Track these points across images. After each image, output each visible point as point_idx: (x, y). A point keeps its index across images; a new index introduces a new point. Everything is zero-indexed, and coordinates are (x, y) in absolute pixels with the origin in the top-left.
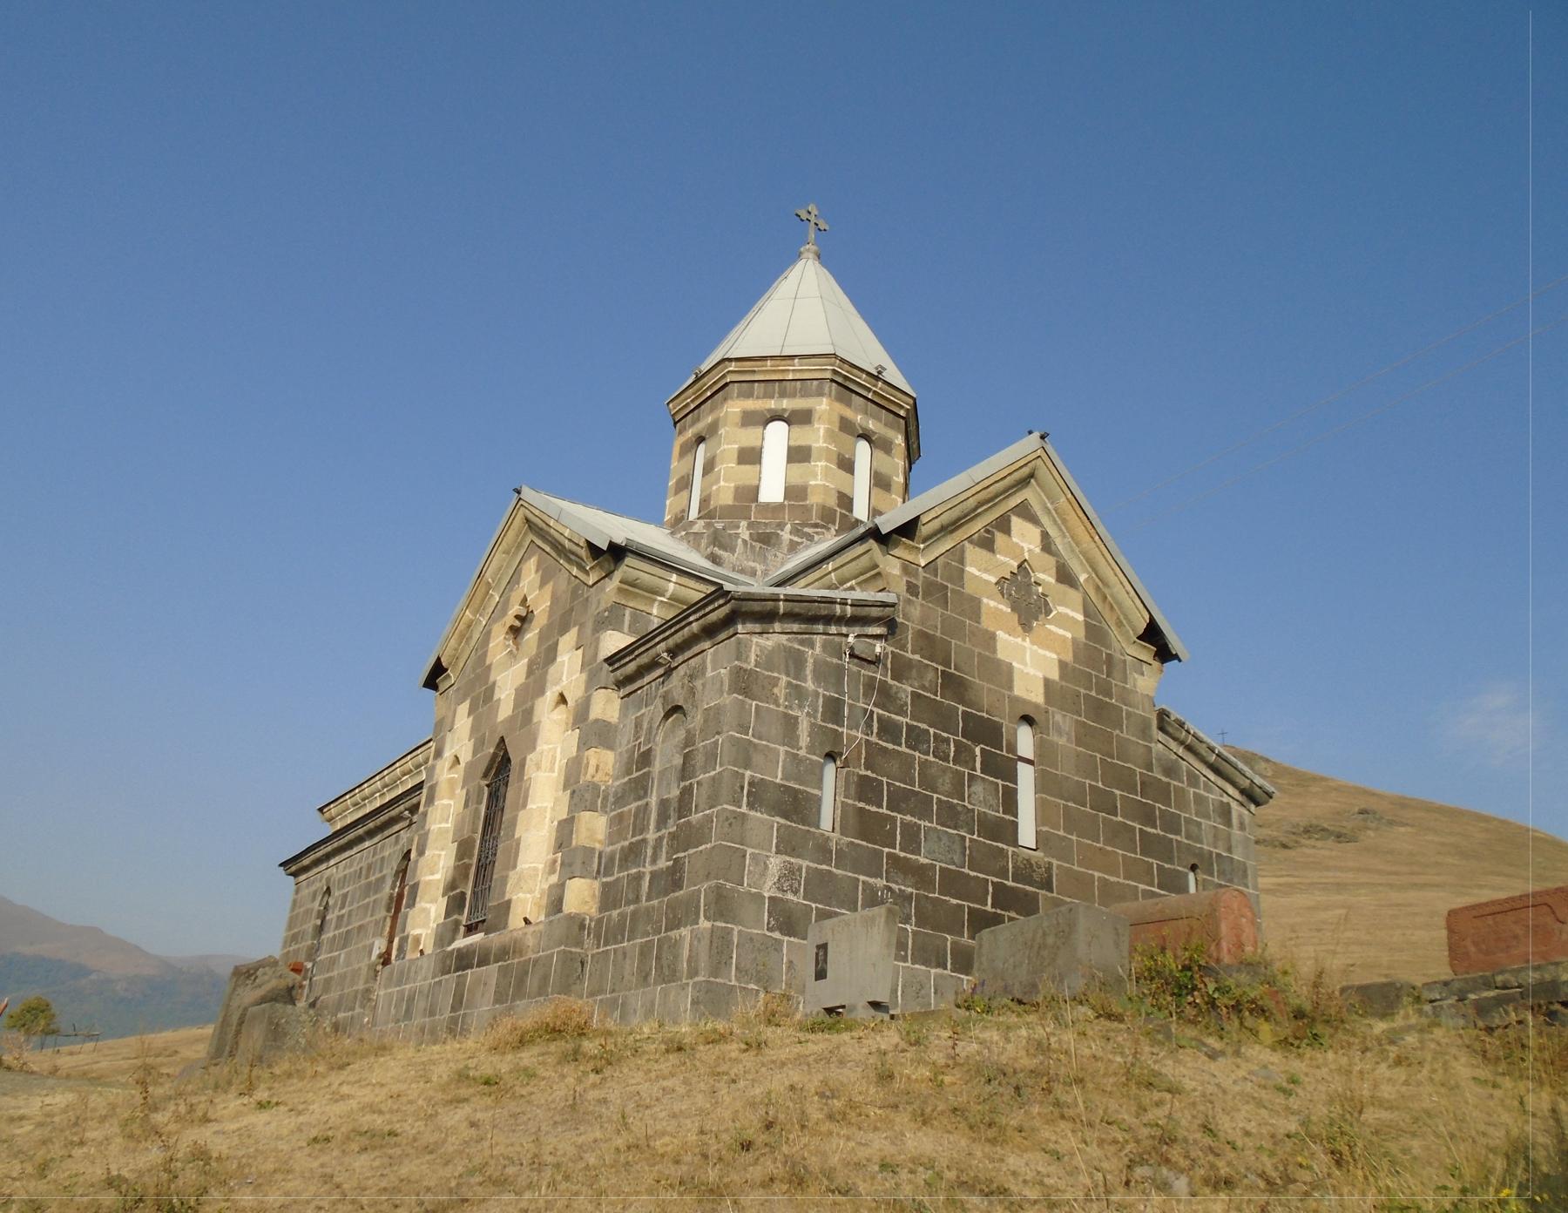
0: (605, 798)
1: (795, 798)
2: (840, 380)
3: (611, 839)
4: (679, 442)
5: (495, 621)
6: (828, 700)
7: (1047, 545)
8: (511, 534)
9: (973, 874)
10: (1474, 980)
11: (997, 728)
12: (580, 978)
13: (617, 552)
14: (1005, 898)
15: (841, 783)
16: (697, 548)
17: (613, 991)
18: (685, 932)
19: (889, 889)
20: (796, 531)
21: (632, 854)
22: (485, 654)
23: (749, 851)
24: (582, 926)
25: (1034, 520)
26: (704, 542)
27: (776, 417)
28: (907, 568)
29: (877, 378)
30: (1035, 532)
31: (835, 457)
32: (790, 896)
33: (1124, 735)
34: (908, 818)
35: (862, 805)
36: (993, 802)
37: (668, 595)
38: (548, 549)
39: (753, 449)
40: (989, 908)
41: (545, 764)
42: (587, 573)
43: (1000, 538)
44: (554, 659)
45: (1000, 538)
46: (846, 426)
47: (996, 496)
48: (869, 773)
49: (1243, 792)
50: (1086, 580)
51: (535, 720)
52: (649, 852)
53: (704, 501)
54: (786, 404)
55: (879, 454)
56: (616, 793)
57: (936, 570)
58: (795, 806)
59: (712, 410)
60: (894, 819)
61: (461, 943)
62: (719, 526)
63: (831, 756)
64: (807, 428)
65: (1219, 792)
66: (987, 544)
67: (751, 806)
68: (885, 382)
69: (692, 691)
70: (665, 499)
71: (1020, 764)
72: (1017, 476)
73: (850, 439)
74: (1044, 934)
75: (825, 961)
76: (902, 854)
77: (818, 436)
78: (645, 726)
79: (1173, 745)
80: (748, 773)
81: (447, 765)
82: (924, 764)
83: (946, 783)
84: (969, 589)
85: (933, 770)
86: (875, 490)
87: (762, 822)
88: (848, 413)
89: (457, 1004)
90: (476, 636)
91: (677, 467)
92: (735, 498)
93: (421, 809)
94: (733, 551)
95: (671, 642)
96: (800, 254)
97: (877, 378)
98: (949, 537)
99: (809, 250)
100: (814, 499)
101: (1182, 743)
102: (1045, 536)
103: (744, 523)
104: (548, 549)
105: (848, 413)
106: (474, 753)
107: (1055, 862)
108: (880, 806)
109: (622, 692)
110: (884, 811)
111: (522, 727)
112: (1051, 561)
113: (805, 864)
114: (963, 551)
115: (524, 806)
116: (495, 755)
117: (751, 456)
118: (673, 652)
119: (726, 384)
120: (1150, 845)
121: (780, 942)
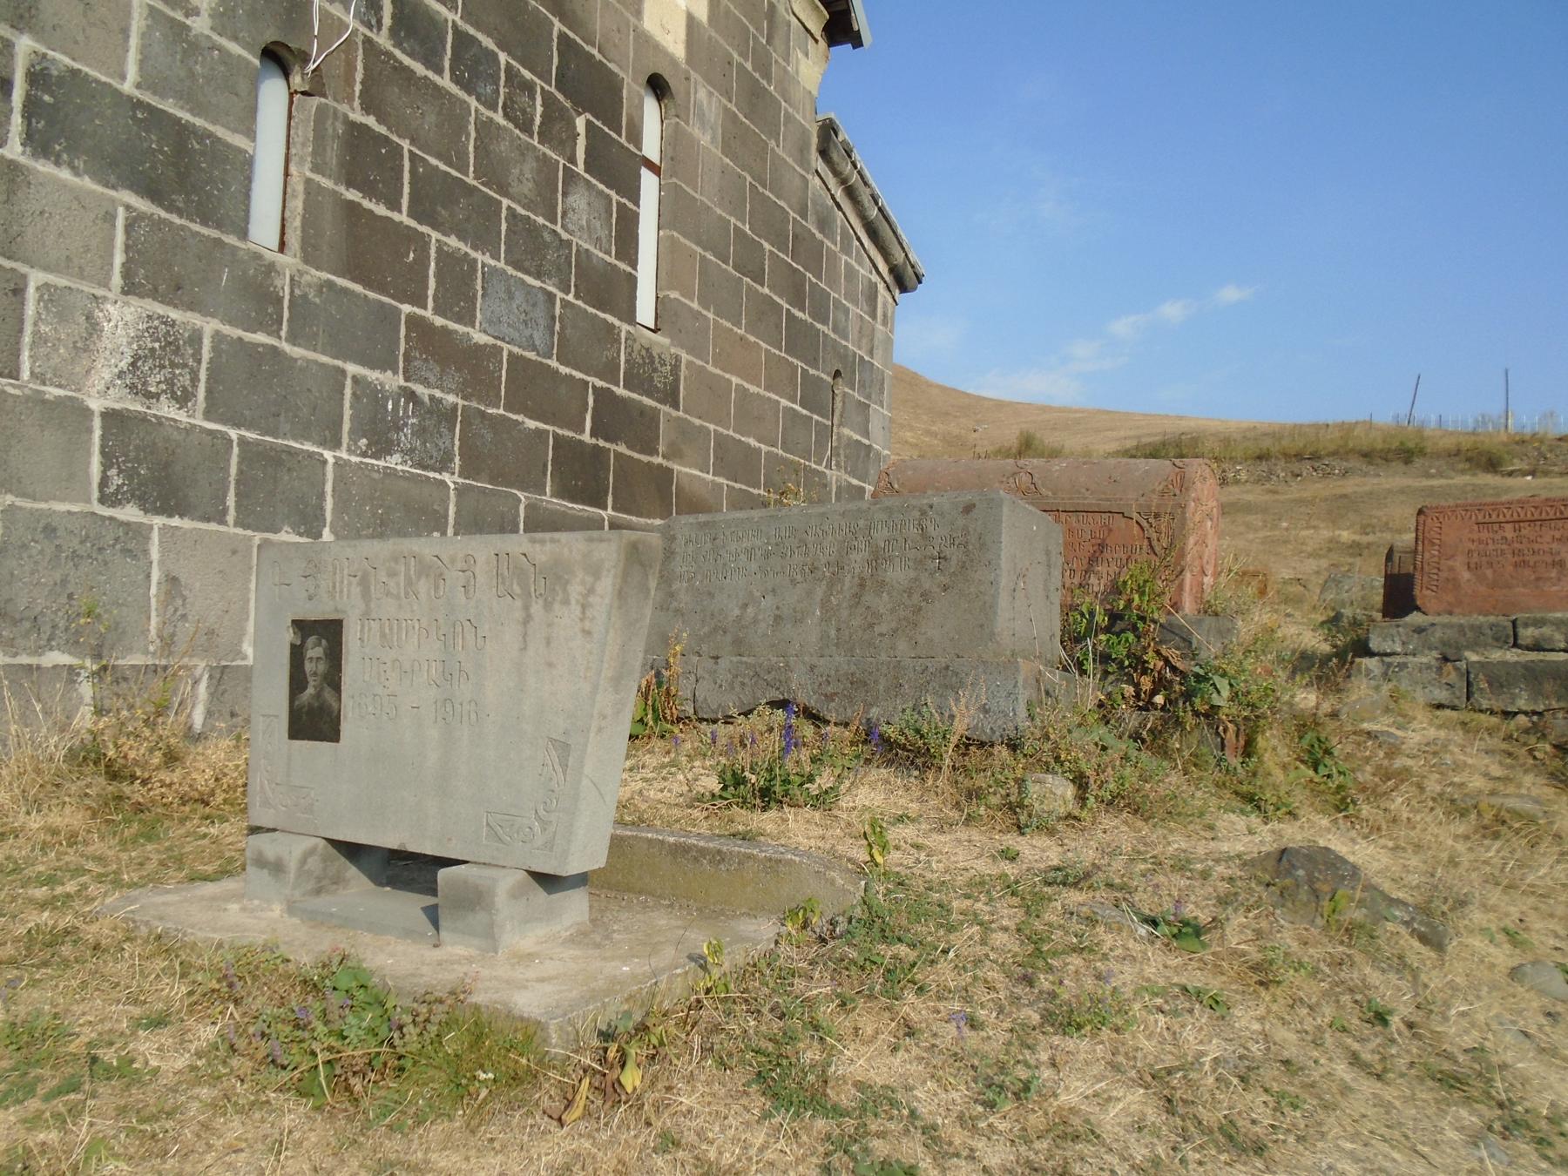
1: (181, 149)
9: (564, 370)
10: (1478, 630)
11: (613, 87)
14: (615, 418)
15: (305, 132)
19: (412, 396)
23: (36, 278)
32: (167, 409)
33: (780, 151)
34: (453, 242)
35: (353, 195)
36: (603, 233)
40: (586, 437)
48: (371, 121)
49: (893, 270)
58: (182, 170)
60: (423, 240)
63: (277, 57)
65: (867, 267)
67: (37, 142)
71: (646, 174)
74: (877, 558)
75: (333, 679)
76: (439, 321)
79: (832, 182)
80: (25, 45)
82: (485, 127)
83: (524, 177)
85: (504, 147)
87: (78, 196)
101: (843, 181)
107: (685, 356)
108: (396, 207)
110: (403, 218)
113: (210, 326)
120: (802, 341)
121: (139, 533)
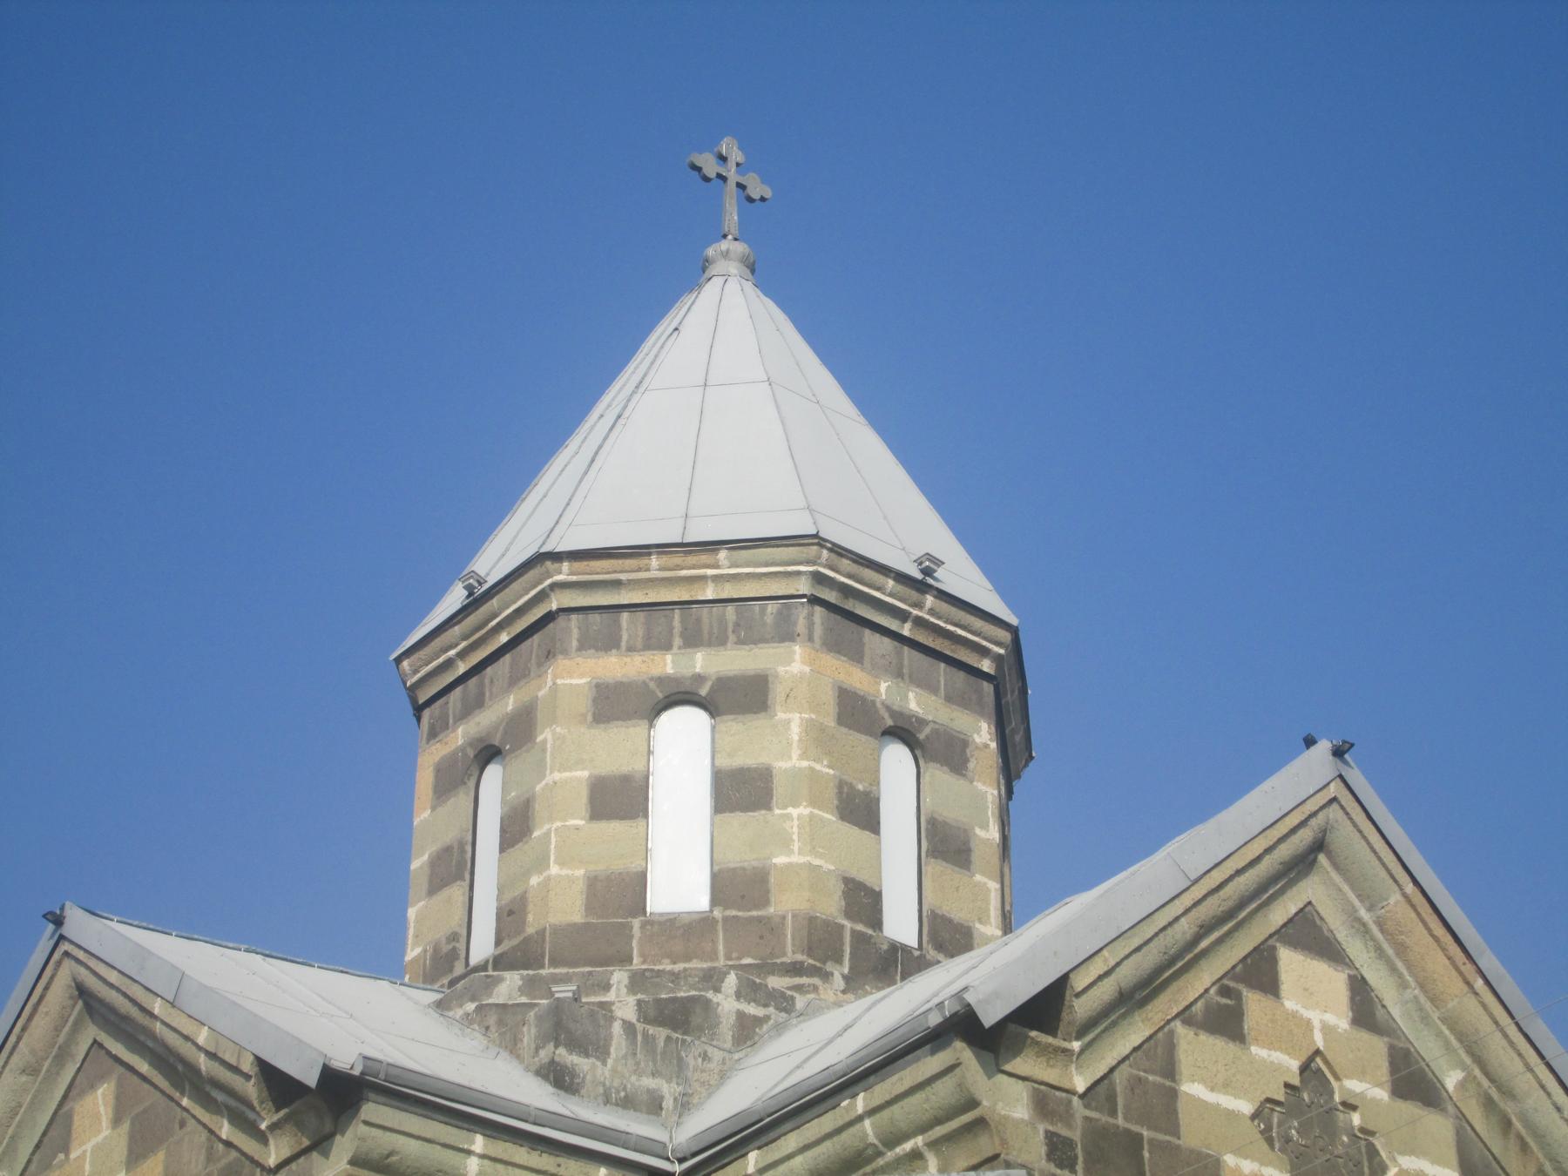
2: (831, 596)
4: (430, 757)
7: (1365, 1009)
8: (41, 1025)
13: (340, 1094)
16: (511, 1045)
20: (750, 990)
25: (1329, 950)
26: (529, 1034)
27: (679, 695)
28: (1047, 1101)
29: (921, 587)
30: (1334, 981)
31: (831, 793)
38: (144, 1067)
39: (626, 779)
42: (262, 1138)
43: (1254, 1004)
45: (1254, 1004)
46: (854, 711)
47: (1241, 905)
50: (1461, 1085)
53: (510, 915)
54: (702, 663)
55: (937, 775)
57: (1111, 1098)
59: (514, 681)
62: (564, 991)
64: (757, 723)
66: (1225, 1021)
68: (943, 595)
70: (405, 911)
72: (1285, 851)
73: (860, 742)
77: (786, 741)
84: (1191, 1136)
86: (933, 867)
88: (857, 679)
91: (431, 823)
92: (589, 908)
94: (598, 1049)
96: (705, 264)
97: (921, 587)
98: (1137, 1017)
99: (727, 254)
100: (787, 903)
102: (1360, 990)
103: (619, 977)
105: (857, 679)
112: (1377, 1047)
114: (1171, 1047)
117: (622, 798)
119: (549, 617)
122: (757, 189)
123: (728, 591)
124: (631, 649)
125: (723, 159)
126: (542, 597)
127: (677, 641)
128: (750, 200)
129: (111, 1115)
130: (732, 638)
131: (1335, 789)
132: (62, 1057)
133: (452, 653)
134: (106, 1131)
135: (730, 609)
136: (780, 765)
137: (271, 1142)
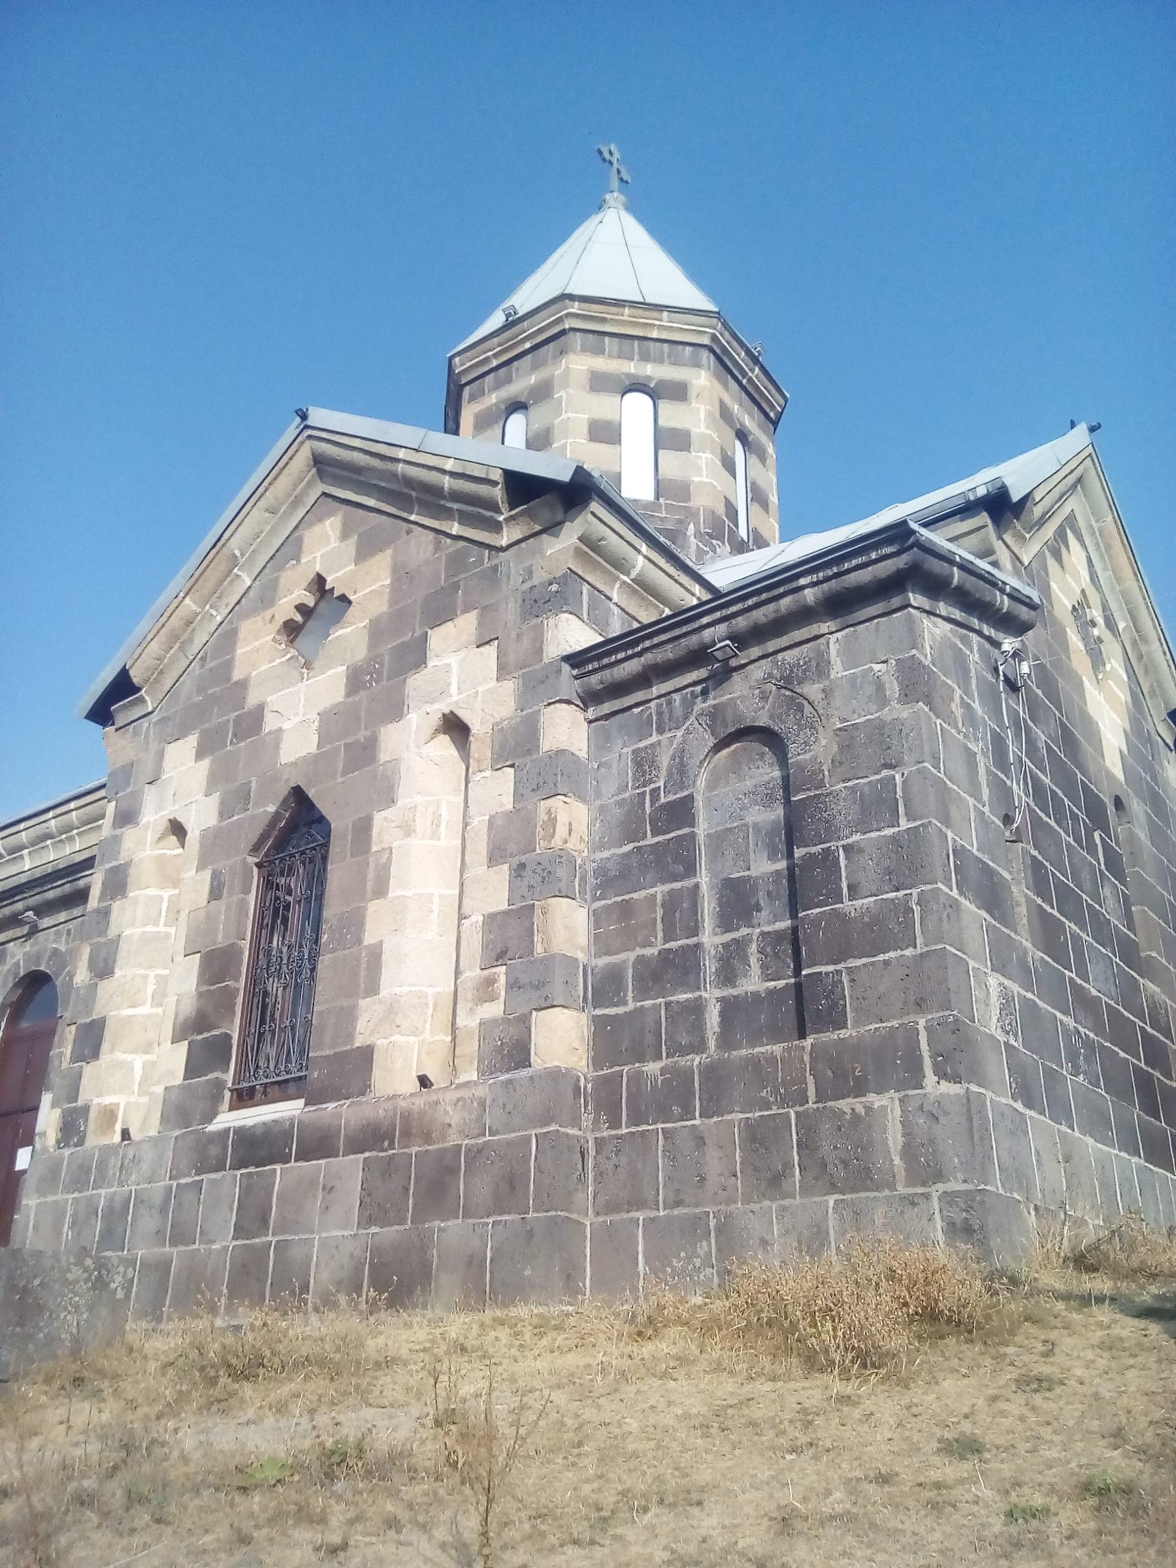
0: (583, 879)
3: (601, 944)
5: (246, 615)
6: (993, 731)
12: (582, 1179)
17: (678, 1203)
18: (886, 1104)
21: (678, 967)
22: (228, 665)
23: (972, 964)
24: (577, 1090)
37: (633, 574)
41: (422, 824)
44: (422, 661)
50: (1124, 629)
51: (383, 757)
52: (710, 966)
54: (652, 371)
55: (754, 460)
56: (600, 872)
59: (535, 367)
61: (228, 1119)
64: (681, 407)
69: (796, 704)
78: (664, 761)
81: (150, 836)
84: (1057, 612)
89: (253, 1216)
90: (201, 637)
93: (93, 902)
95: (741, 623)
99: (615, 199)
104: (371, 502)
106: (225, 812)
109: (591, 713)
111: (344, 774)
115: (381, 890)
116: (277, 816)
117: (606, 433)
118: (741, 640)
119: (563, 333)
122: (625, 176)
123: (665, 336)
124: (610, 356)
125: (611, 154)
126: (559, 320)
127: (636, 357)
128: (621, 180)
129: (338, 533)
130: (667, 361)
131: (1090, 450)
132: (296, 502)
133: (490, 354)
134: (334, 543)
135: (666, 345)
136: (695, 431)
137: (505, 529)
